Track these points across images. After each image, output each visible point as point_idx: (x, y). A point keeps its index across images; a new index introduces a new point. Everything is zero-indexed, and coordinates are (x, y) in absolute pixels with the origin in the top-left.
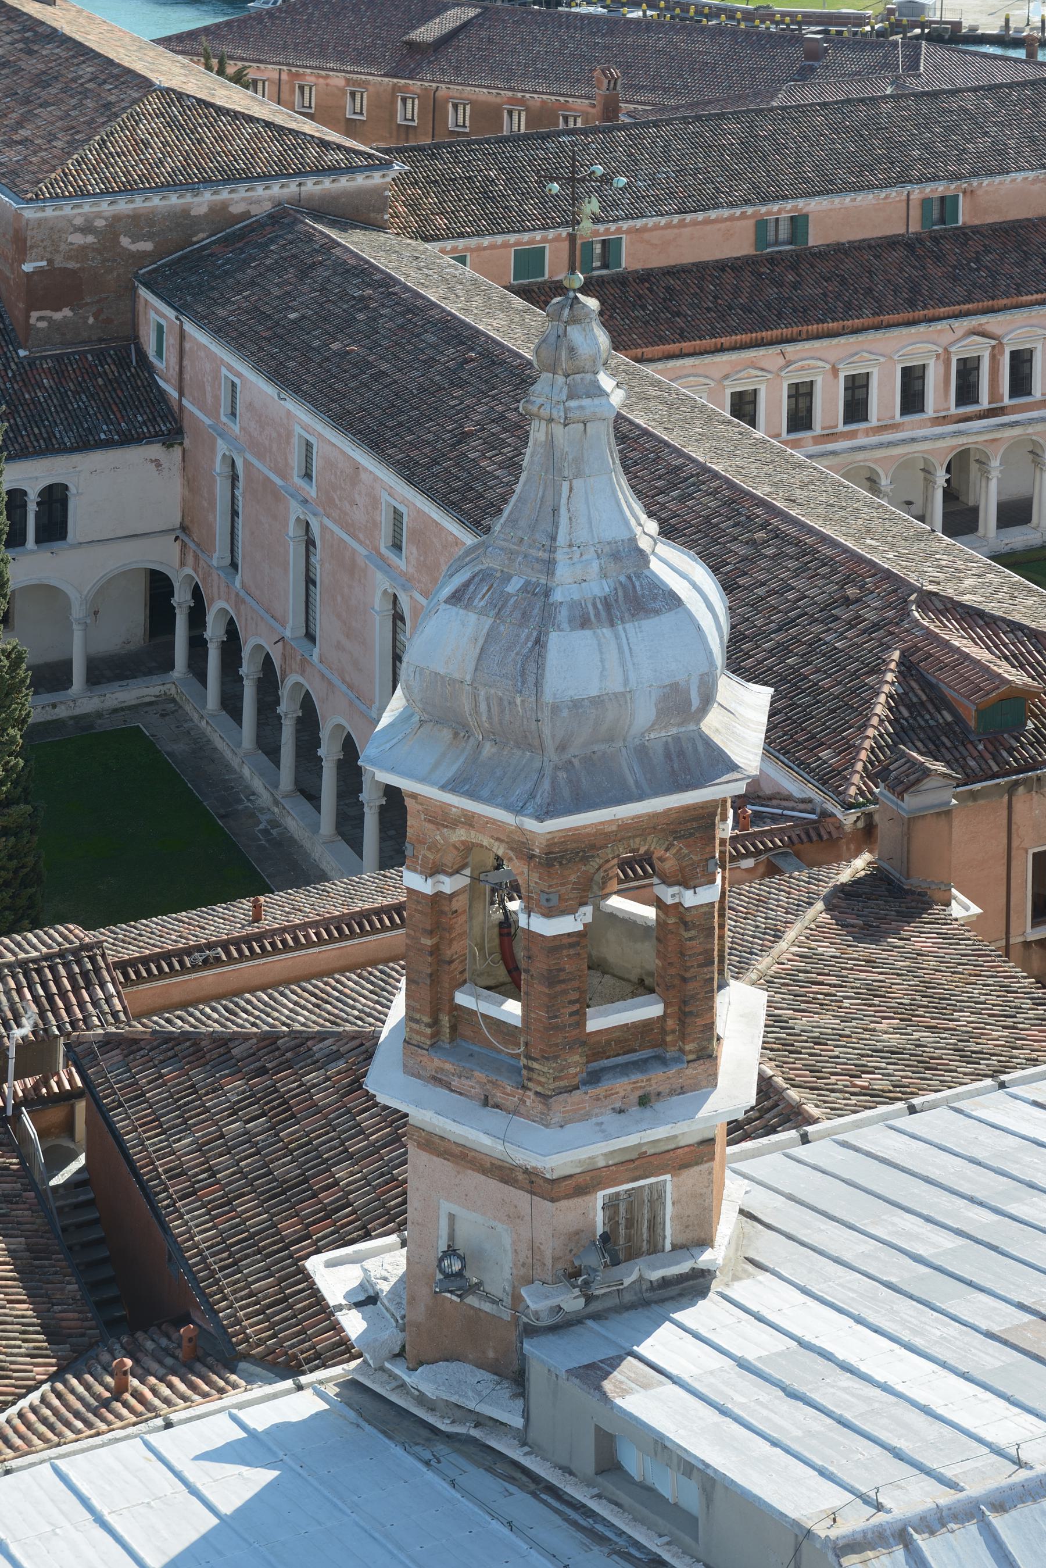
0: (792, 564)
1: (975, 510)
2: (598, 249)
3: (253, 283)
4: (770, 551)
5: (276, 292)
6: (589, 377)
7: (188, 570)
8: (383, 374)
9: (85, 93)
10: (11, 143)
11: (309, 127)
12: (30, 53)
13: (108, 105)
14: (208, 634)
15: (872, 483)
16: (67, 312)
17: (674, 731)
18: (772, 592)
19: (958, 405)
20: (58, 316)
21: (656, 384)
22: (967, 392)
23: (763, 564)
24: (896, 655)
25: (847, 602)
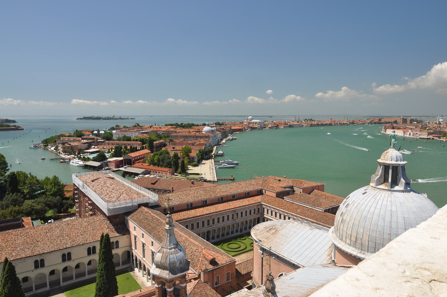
1: (209, 238)
2: (172, 208)
3: (136, 214)
4: (190, 244)
5: (139, 215)
6: (171, 224)
8: (150, 225)
10: (110, 198)
12: (111, 186)
13: (120, 192)
14: (134, 258)
17: (181, 266)
18: (190, 249)
21: (178, 225)
22: (208, 224)
23: (189, 246)
25: (198, 249)
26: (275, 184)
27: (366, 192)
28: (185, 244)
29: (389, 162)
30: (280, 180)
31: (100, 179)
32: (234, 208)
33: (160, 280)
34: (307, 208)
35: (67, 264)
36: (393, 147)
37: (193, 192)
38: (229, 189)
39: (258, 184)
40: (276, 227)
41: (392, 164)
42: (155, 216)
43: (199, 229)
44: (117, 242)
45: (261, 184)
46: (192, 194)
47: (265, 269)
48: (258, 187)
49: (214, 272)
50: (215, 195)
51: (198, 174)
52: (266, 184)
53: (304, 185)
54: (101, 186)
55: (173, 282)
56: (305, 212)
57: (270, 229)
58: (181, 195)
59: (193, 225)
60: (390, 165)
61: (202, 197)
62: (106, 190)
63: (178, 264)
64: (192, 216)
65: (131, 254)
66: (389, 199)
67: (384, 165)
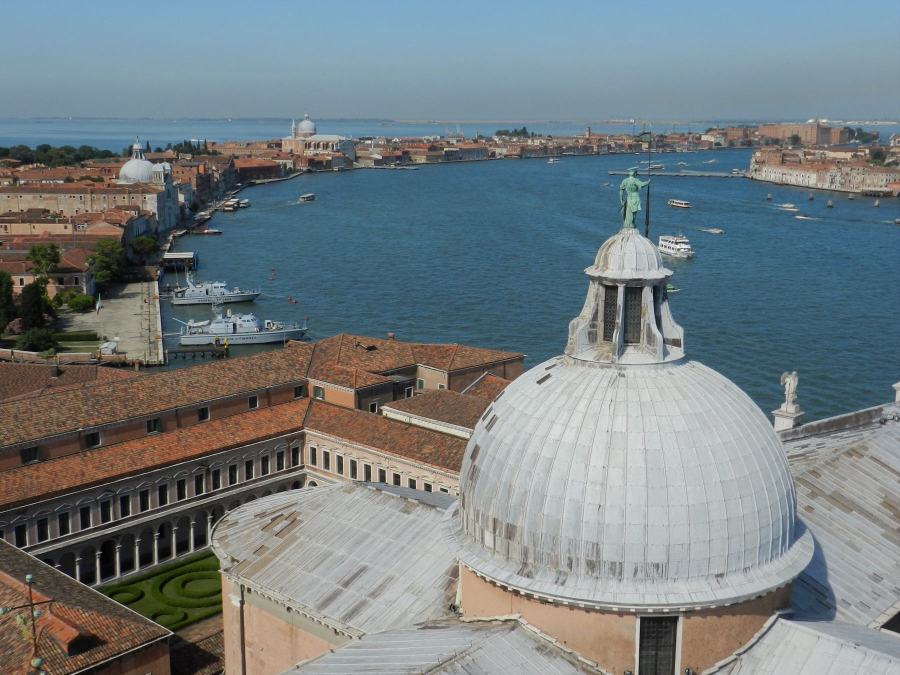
26: (356, 361)
27: (548, 376)
29: (612, 273)
30: (372, 348)
32: (201, 455)
34: (455, 439)
36: (632, 225)
37: (45, 405)
38: (184, 388)
39: (294, 366)
40: (294, 510)
41: (622, 281)
45: (305, 365)
46: (39, 412)
47: (252, 655)
48: (293, 375)
50: (129, 413)
52: (322, 364)
53: (453, 360)
56: (449, 454)
57: (273, 520)
60: (618, 285)
64: (37, 494)
66: (609, 396)
67: (605, 283)
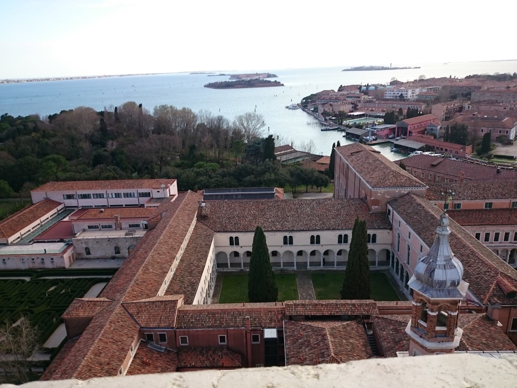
0: (480, 264)
3: (403, 205)
4: (477, 261)
5: (407, 207)
7: (392, 250)
8: (421, 223)
9: (382, 170)
10: (371, 178)
11: (414, 178)
12: (375, 162)
15: (497, 252)
16: (377, 207)
18: (477, 268)
19: (514, 240)
20: (376, 207)
21: (463, 230)
23: (476, 263)
24: (495, 282)
25: (488, 272)
28: (469, 260)
31: (362, 153)
33: (420, 298)
35: (315, 247)
42: (429, 212)
43: (498, 243)
44: (374, 236)
46: (494, 188)
49: (512, 311)
51: (511, 158)
54: (362, 161)
55: (438, 305)
58: (475, 188)
59: (487, 235)
61: (511, 195)
62: (367, 168)
63: (448, 284)
65: (391, 255)
